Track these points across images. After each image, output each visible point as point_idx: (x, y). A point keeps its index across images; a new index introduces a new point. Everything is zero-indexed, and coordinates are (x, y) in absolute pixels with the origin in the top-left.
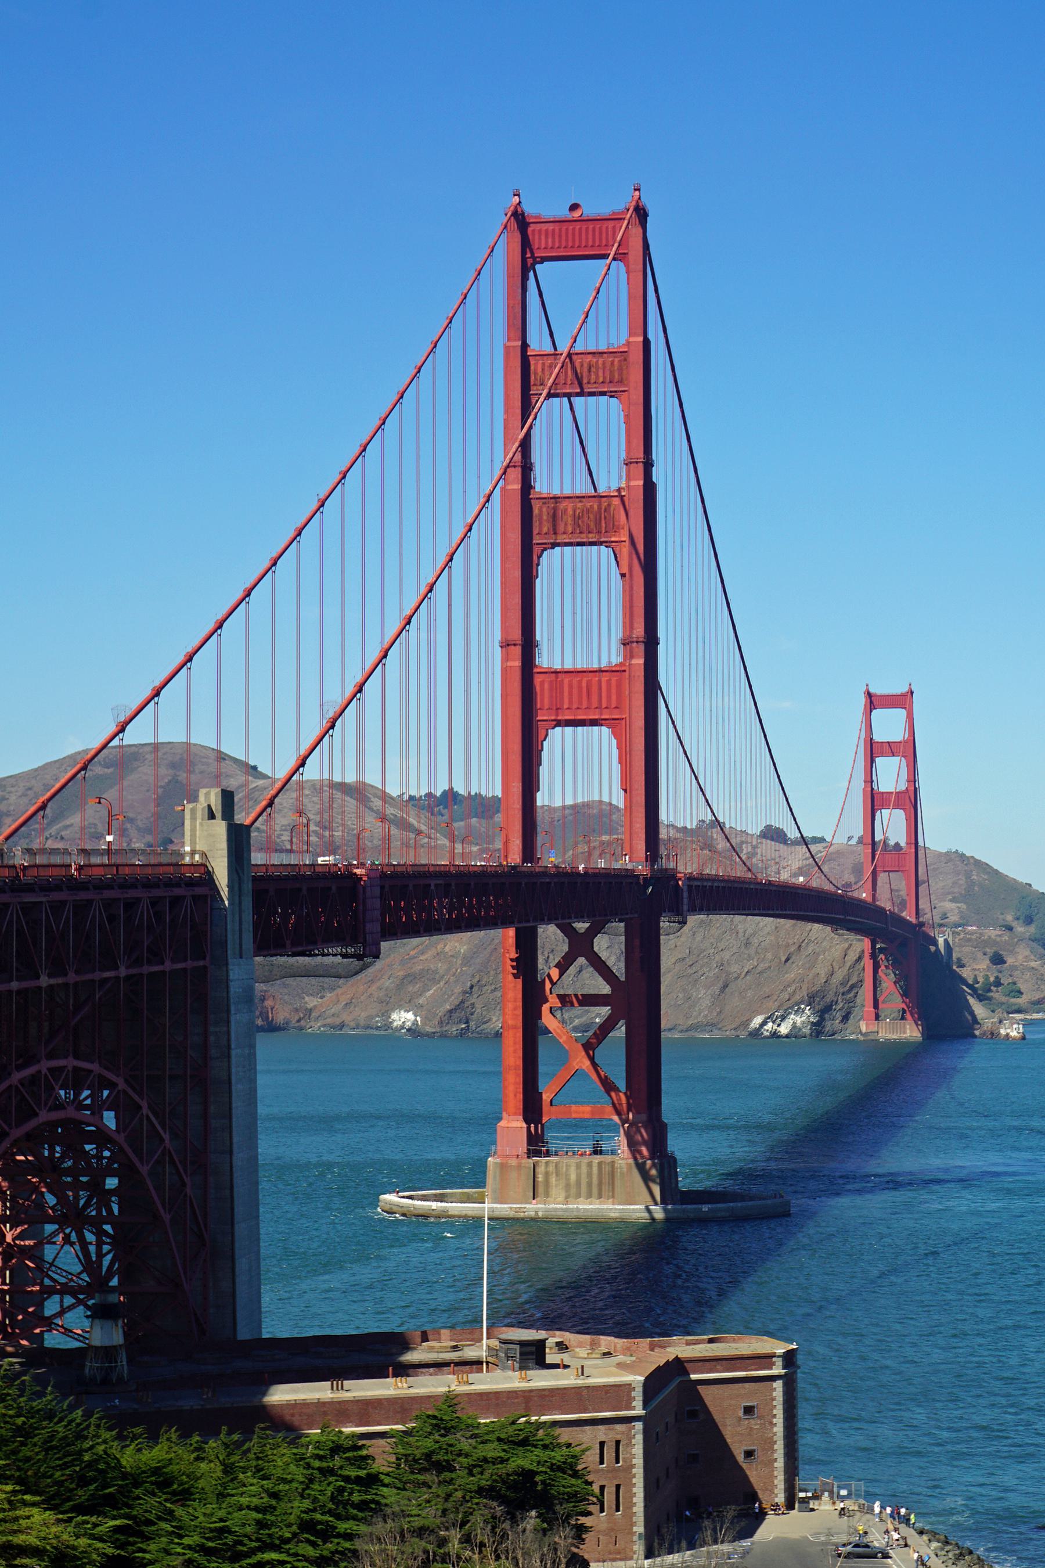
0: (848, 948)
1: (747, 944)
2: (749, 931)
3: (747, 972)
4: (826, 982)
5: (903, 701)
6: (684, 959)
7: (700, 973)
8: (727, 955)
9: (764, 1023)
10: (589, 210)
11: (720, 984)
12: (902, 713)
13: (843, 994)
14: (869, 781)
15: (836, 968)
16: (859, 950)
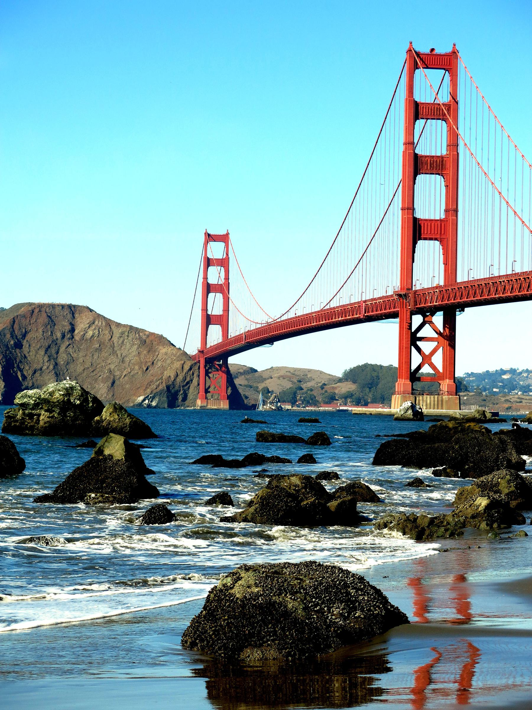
0: (184, 363)
1: (123, 361)
2: (124, 354)
4: (174, 380)
5: (224, 238)
6: (88, 368)
7: (99, 375)
8: (112, 367)
10: (438, 51)
11: (111, 381)
12: (222, 245)
13: (183, 386)
14: (205, 278)
15: (179, 373)
16: (189, 364)
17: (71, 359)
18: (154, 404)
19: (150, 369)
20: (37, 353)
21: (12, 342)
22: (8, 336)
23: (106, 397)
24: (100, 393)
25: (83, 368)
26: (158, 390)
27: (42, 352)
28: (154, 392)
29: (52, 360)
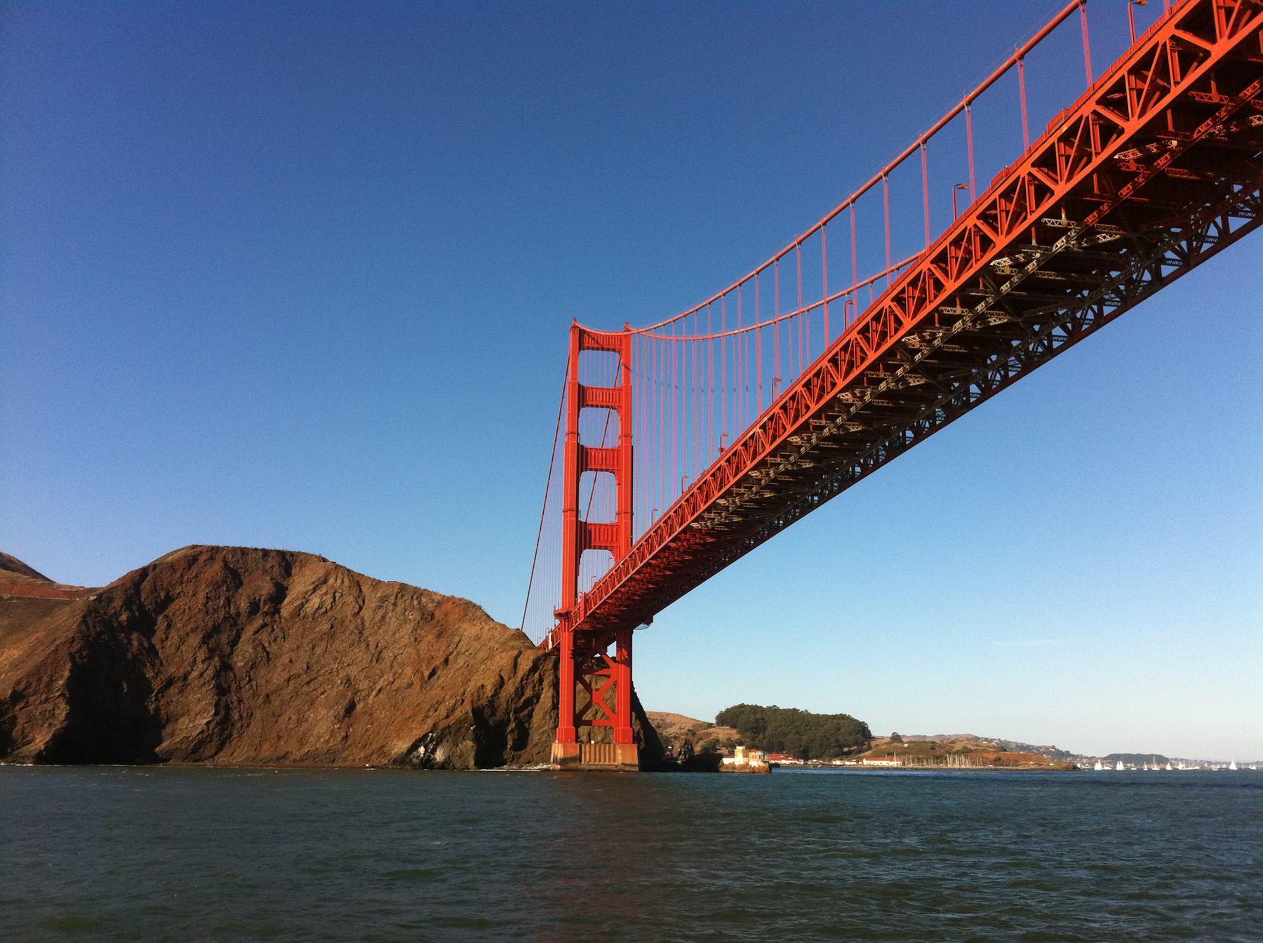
3: (380, 691)
7: (321, 690)
8: (353, 671)
9: (415, 747)
15: (506, 678)
17: (261, 657)
18: (439, 756)
19: (439, 672)
20: (182, 641)
21: (124, 617)
22: (118, 603)
23: (327, 742)
24: (315, 733)
25: (286, 676)
26: (452, 720)
27: (195, 640)
28: (441, 726)
29: (216, 659)
